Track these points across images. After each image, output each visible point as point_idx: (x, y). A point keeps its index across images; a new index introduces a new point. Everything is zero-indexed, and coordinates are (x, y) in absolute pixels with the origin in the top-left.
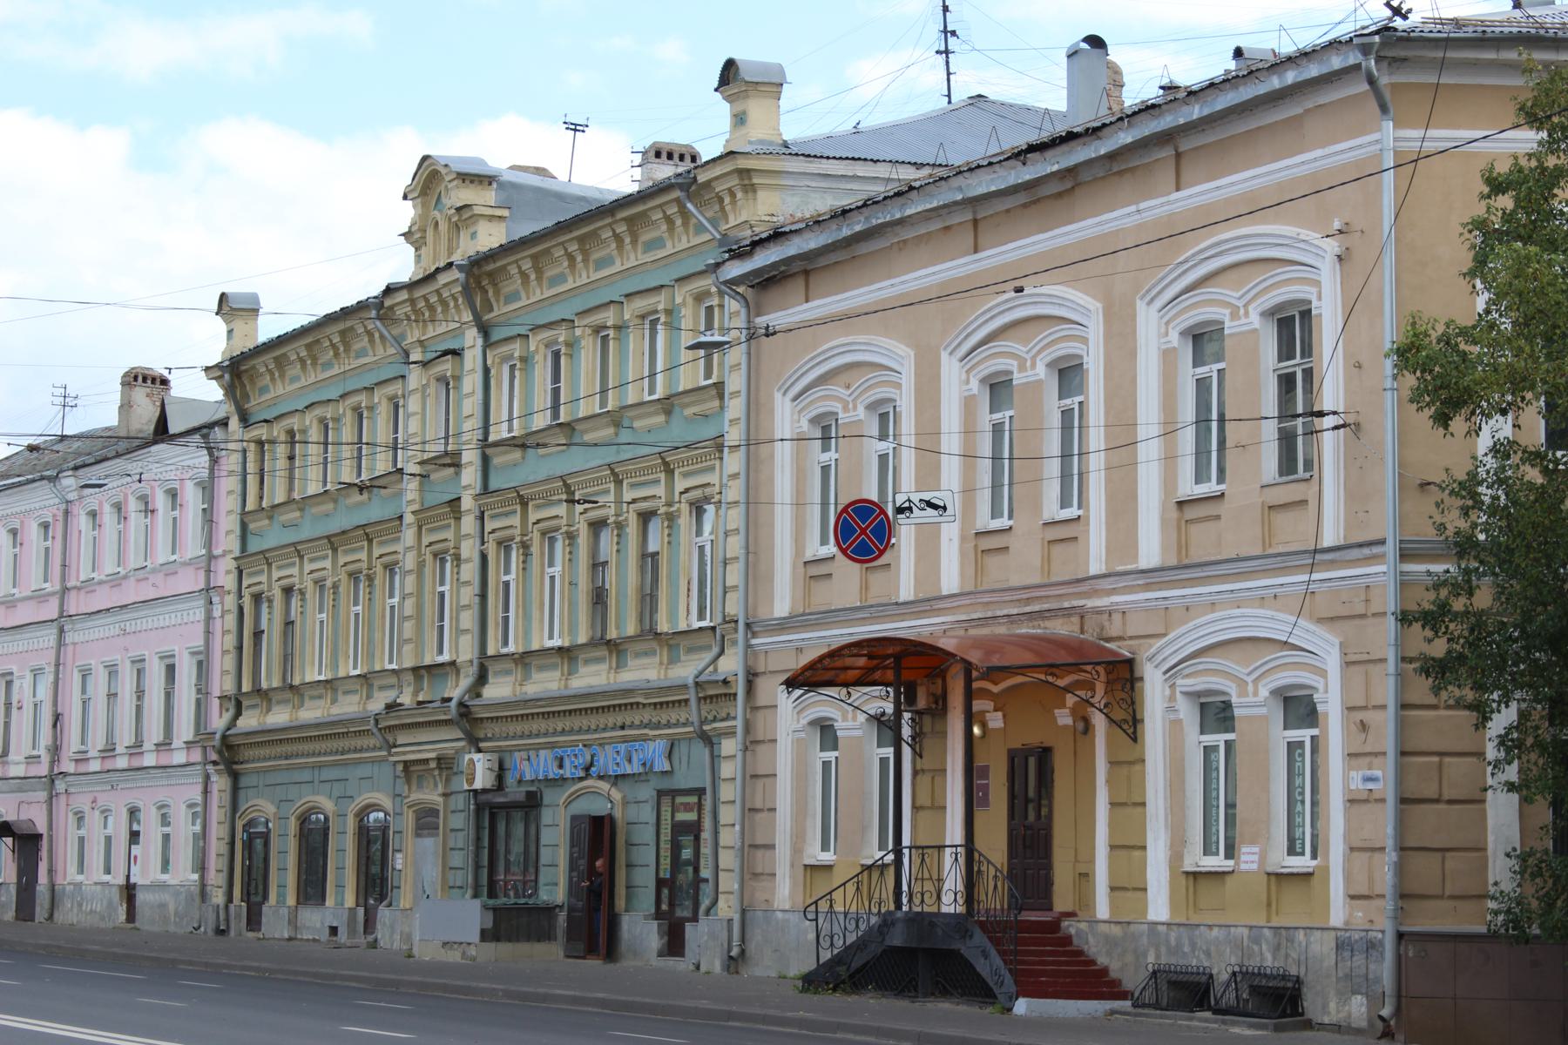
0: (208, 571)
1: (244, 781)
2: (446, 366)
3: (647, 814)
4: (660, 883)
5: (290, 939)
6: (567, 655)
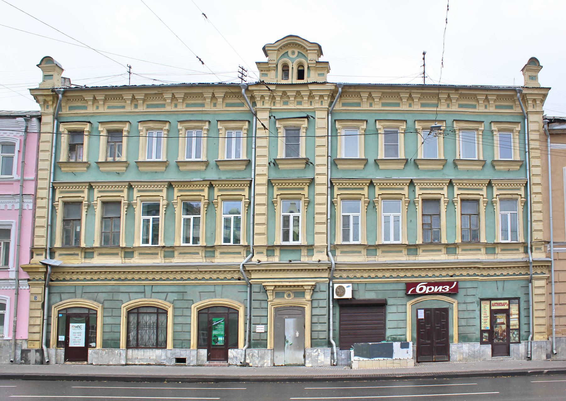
0: (22, 186)
1: (54, 290)
2: (304, 124)
3: (475, 307)
4: (482, 332)
5: (126, 365)
6: (412, 248)
